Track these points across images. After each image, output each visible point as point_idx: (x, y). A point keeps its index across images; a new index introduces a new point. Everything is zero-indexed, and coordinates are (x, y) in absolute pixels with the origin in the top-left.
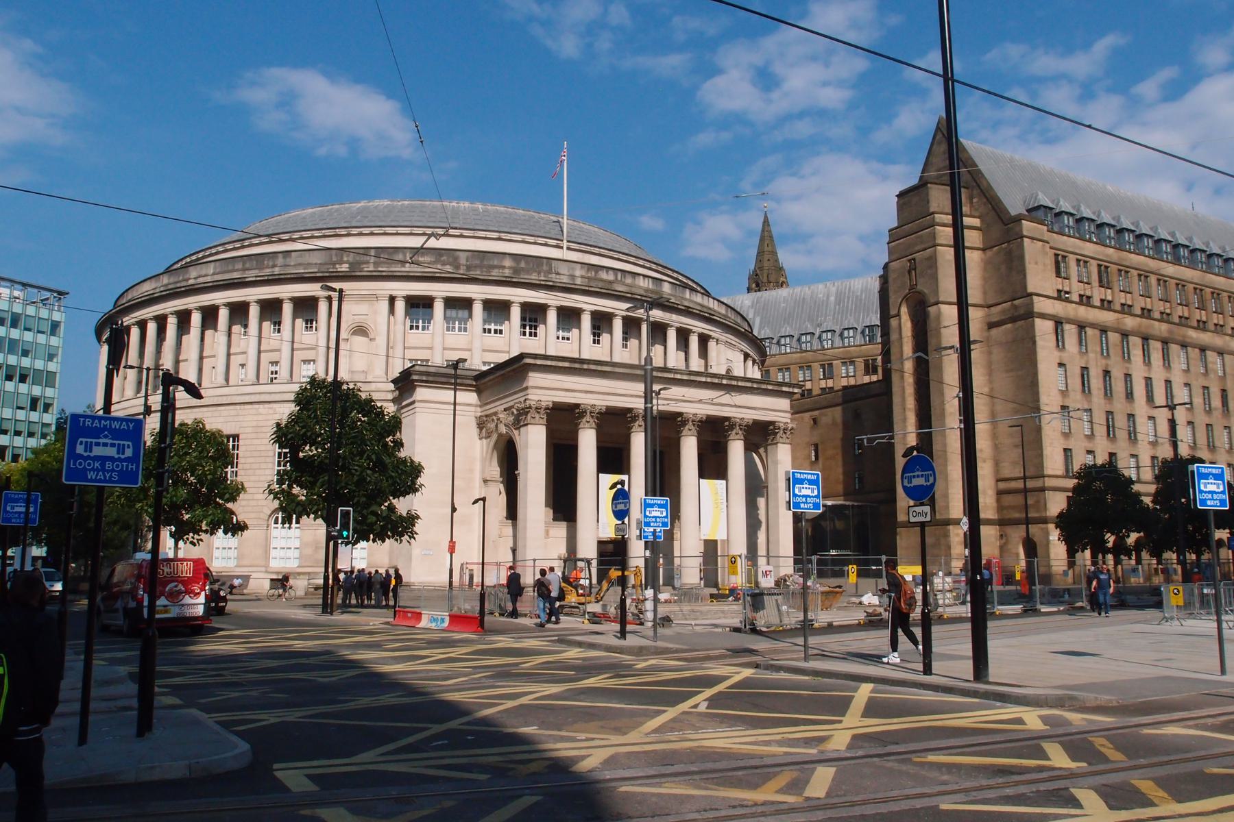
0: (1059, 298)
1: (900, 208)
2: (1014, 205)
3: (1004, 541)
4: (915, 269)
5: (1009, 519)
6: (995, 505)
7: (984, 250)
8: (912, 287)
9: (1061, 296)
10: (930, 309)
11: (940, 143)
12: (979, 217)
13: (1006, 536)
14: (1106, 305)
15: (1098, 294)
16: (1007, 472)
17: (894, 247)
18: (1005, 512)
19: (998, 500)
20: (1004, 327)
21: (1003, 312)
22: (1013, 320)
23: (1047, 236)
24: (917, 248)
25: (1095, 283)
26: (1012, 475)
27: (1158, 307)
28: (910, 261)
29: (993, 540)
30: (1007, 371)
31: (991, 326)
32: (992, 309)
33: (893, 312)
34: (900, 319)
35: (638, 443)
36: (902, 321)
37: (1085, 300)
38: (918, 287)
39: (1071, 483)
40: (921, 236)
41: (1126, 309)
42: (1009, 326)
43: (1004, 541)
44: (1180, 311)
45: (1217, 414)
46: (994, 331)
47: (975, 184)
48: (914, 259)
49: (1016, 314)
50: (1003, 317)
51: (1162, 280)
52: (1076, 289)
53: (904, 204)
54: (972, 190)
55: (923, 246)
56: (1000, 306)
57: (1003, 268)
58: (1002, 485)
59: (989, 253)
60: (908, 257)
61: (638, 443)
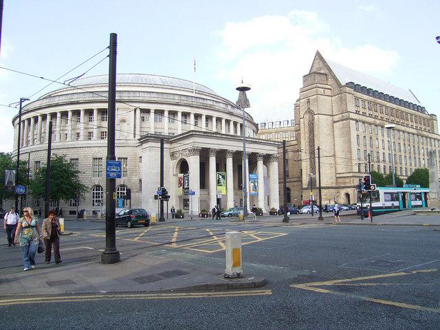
0: (356, 113)
1: (304, 81)
2: (343, 82)
9: (357, 113)
14: (370, 116)
15: (368, 112)
16: (339, 171)
22: (342, 120)
23: (353, 92)
25: (367, 109)
27: (385, 117)
35: (229, 162)
37: (364, 114)
39: (406, 178)
41: (376, 117)
44: (380, 115)
45: (403, 152)
51: (387, 107)
52: (361, 111)
57: (339, 103)
58: (338, 176)
61: (229, 162)
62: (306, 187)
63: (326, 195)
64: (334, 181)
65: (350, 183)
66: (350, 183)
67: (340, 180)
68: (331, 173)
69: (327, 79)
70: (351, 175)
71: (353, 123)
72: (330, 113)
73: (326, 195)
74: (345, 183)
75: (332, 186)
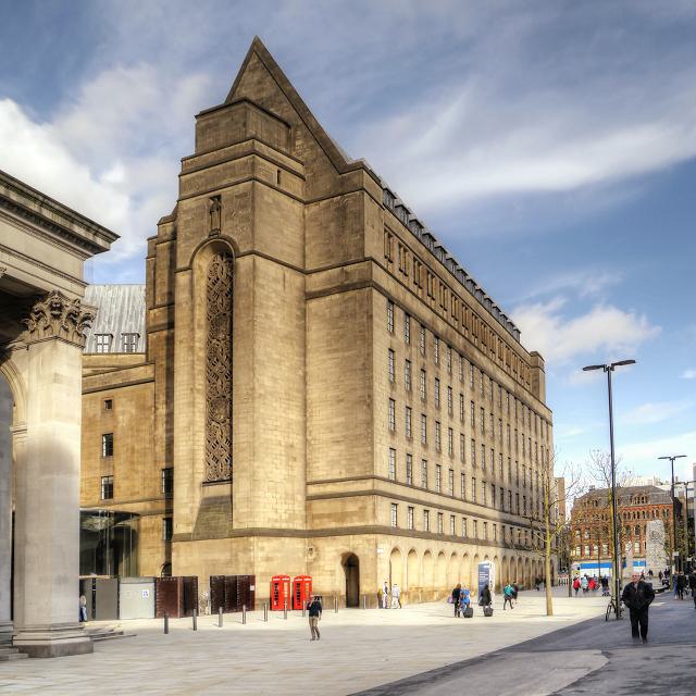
1: (201, 132)
3: (314, 556)
4: (219, 209)
5: (323, 530)
6: (303, 513)
7: (305, 203)
8: (215, 232)
10: (239, 260)
11: (253, 71)
12: (302, 164)
13: (317, 549)
16: (321, 472)
17: (187, 181)
18: (317, 521)
19: (307, 508)
20: (328, 298)
21: (329, 280)
22: (343, 289)
24: (225, 182)
26: (329, 478)
28: (212, 198)
29: (301, 555)
30: (329, 352)
31: (310, 296)
32: (314, 275)
33: (181, 264)
34: (192, 274)
36: (195, 276)
38: (223, 233)
40: (233, 167)
42: (337, 296)
43: (314, 556)
46: (313, 304)
47: (300, 122)
48: (219, 197)
49: (347, 282)
50: (329, 286)
53: (208, 126)
54: (296, 130)
55: (233, 180)
56: (325, 273)
57: (333, 226)
58: (313, 490)
59: (314, 208)
60: (212, 194)
62: (191, 529)
63: (268, 559)
64: (299, 507)
65: (362, 517)
66: (362, 517)
67: (321, 507)
68: (290, 479)
69: (290, 141)
70: (368, 486)
71: (379, 301)
72: (296, 262)
73: (268, 559)
74: (343, 516)
75: (291, 526)
